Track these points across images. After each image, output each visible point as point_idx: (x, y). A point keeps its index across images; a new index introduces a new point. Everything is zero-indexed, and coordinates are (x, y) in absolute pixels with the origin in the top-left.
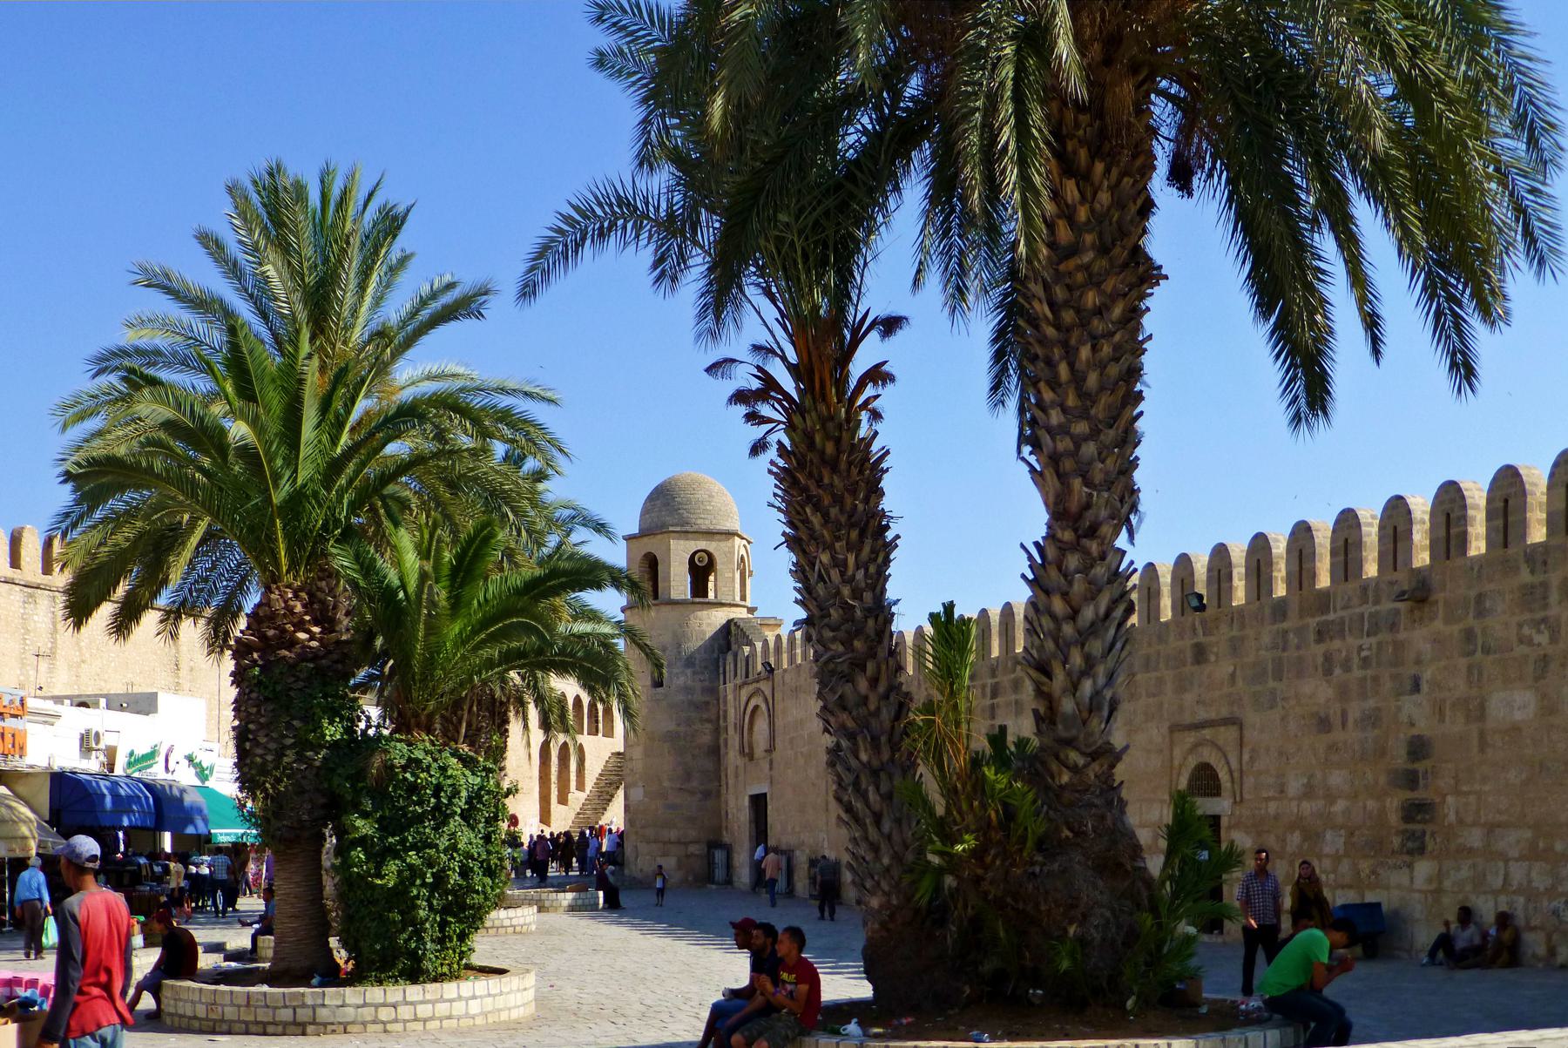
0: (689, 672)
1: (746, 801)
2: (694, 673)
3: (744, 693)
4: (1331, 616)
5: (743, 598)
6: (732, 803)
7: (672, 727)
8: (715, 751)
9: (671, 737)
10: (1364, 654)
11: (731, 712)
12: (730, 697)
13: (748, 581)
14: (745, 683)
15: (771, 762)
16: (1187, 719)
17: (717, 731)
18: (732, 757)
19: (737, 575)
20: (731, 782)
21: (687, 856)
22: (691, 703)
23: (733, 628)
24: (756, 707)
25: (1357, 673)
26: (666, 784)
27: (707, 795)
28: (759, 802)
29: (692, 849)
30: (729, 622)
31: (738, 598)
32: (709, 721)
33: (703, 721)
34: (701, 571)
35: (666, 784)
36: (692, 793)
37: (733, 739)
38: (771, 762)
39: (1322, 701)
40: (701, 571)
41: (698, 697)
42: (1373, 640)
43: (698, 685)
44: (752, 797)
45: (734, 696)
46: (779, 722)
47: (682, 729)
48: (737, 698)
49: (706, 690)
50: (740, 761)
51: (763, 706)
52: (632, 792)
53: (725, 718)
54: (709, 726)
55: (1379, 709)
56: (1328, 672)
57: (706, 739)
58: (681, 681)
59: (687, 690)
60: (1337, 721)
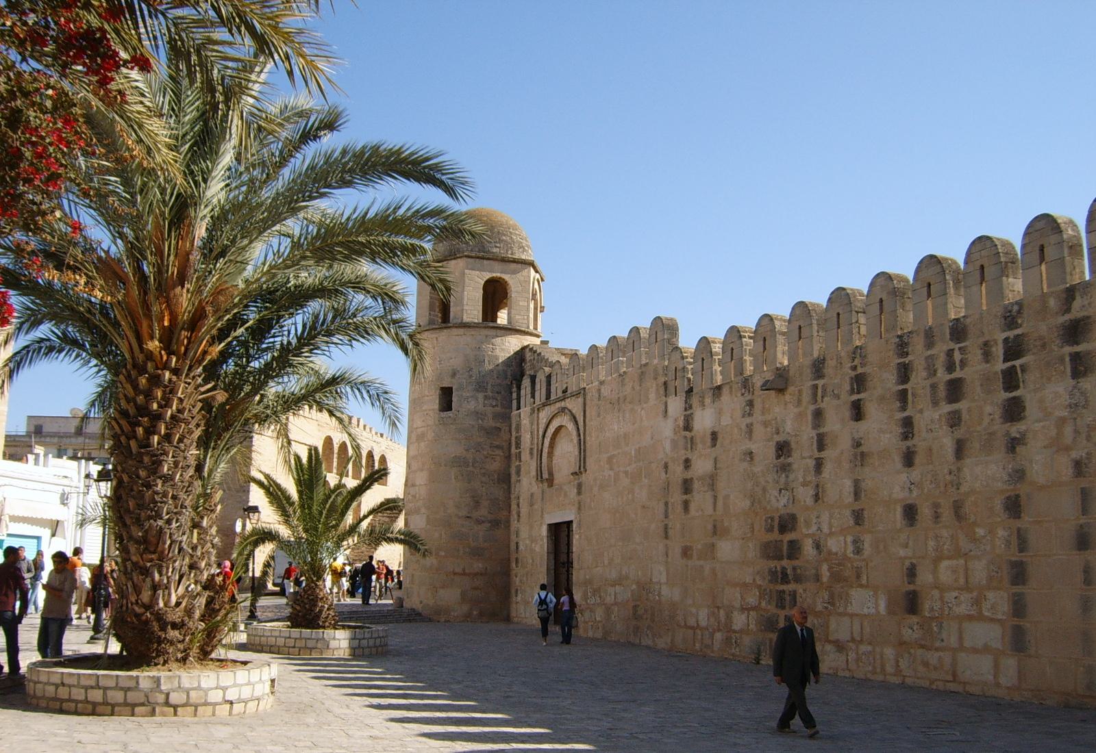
0: (481, 396)
1: (544, 531)
2: (486, 397)
3: (544, 415)
5: (536, 328)
6: (524, 534)
8: (505, 479)
9: (459, 462)
11: (526, 439)
12: (525, 422)
13: (539, 315)
14: (544, 405)
15: (579, 486)
18: (526, 484)
20: (524, 510)
22: (481, 428)
23: (528, 355)
24: (560, 428)
27: (495, 524)
28: (560, 533)
30: (524, 348)
31: (531, 327)
34: (495, 295)
36: (479, 522)
37: (529, 465)
38: (579, 486)
40: (495, 295)
41: (490, 423)
43: (489, 410)
44: (550, 526)
45: (528, 421)
46: (592, 441)
48: (534, 421)
49: (496, 416)
50: (536, 488)
51: (571, 426)
52: (412, 518)
53: (518, 445)
57: (495, 465)
58: (472, 405)
59: (478, 415)
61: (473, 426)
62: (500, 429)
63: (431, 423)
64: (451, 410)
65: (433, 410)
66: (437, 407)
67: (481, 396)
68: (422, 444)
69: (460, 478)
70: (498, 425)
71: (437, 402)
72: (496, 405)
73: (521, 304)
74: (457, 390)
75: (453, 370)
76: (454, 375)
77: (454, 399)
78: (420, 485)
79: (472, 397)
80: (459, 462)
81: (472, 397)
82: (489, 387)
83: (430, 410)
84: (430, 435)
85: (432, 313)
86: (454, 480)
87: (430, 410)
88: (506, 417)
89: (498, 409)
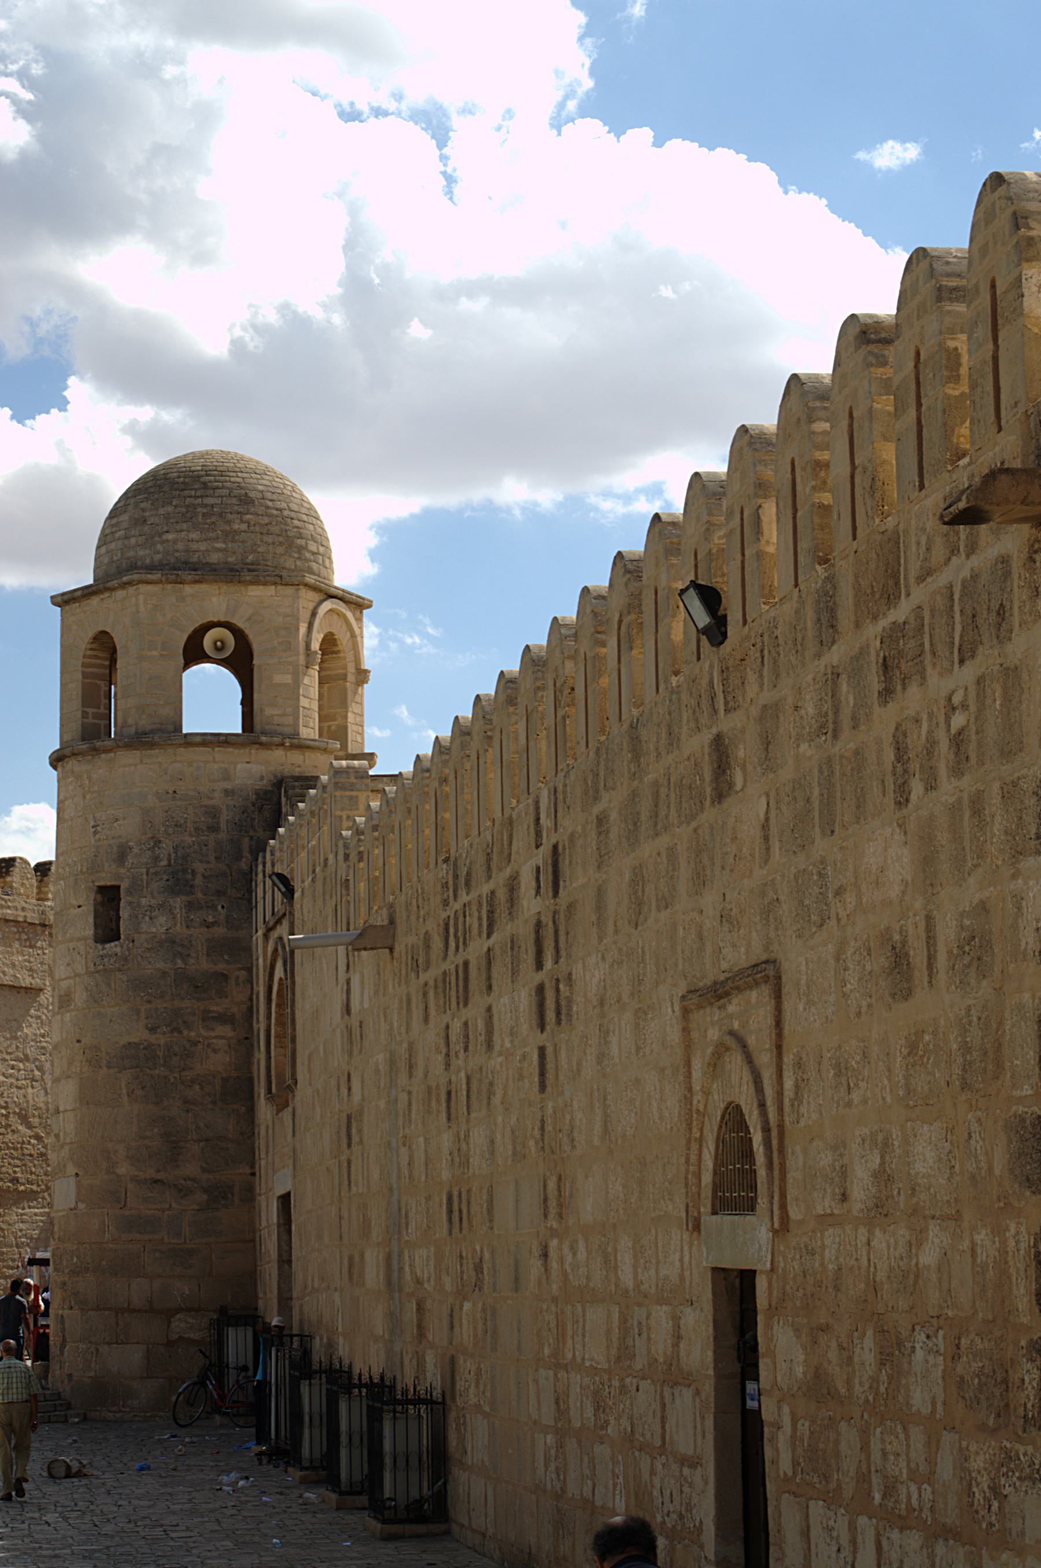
0: (178, 903)
2: (190, 906)
4: (901, 612)
7: (139, 1034)
10: (958, 720)
16: (711, 973)
17: (246, 1042)
19: (311, 680)
21: (170, 1344)
25: (949, 788)
26: (123, 1169)
29: (180, 1325)
32: (223, 1018)
33: (209, 1018)
35: (123, 1169)
39: (894, 892)
41: (202, 964)
42: (967, 674)
44: (279, 1197)
47: (160, 1039)
54: (225, 1030)
55: (983, 908)
56: (902, 800)
57: (217, 1061)
58: (160, 925)
59: (172, 945)
60: (918, 957)
61: (164, 974)
62: (225, 977)
63: (80, 969)
64: (119, 938)
65: (85, 939)
66: (90, 932)
67: (178, 903)
68: (68, 1017)
69: (139, 1092)
70: (221, 967)
71: (91, 920)
72: (214, 924)
73: (278, 679)
74: (129, 892)
75: (121, 846)
76: (121, 856)
77: (124, 913)
78: (66, 1111)
79: (161, 906)
80: (136, 1058)
81: (161, 906)
82: (199, 880)
83: (79, 939)
84: (80, 998)
85: (90, 710)
86: (125, 1098)
87: (79, 939)
88: (239, 950)
89: (220, 931)
